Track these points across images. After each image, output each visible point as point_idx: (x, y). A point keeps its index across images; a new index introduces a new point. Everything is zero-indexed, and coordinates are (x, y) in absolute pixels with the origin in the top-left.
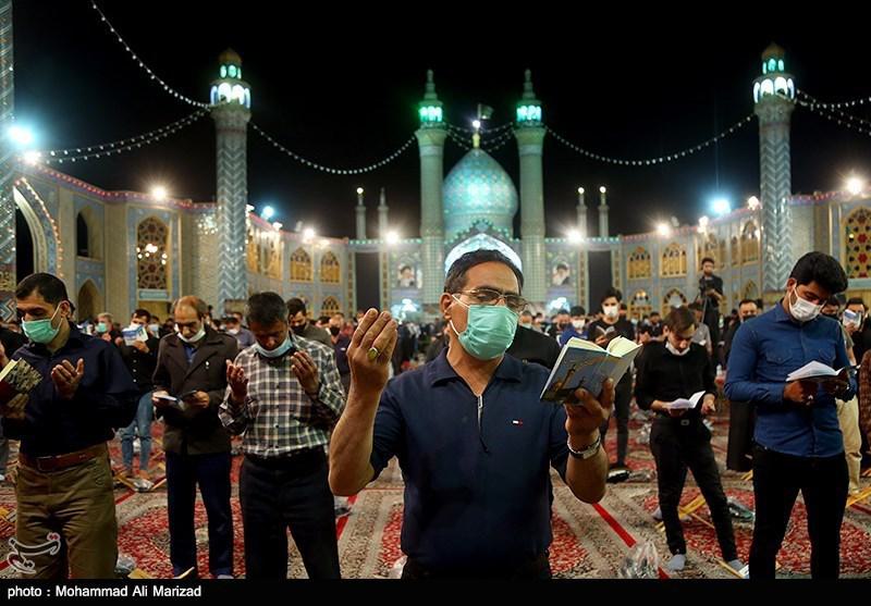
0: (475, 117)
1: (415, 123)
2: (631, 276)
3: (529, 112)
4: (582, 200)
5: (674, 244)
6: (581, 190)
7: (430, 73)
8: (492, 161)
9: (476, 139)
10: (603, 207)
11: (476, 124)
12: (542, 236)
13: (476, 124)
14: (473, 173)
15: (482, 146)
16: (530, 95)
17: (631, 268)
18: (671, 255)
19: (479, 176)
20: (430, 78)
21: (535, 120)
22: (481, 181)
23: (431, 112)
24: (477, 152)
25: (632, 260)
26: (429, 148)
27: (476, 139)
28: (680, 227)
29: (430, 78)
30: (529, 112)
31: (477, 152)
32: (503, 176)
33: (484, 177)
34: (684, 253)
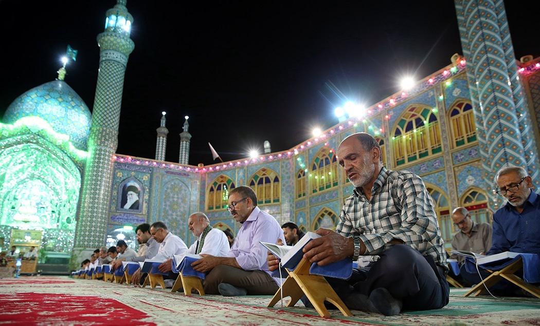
2: (210, 208)
4: (163, 122)
5: (264, 170)
6: (164, 113)
8: (73, 91)
9: (62, 73)
11: (65, 60)
12: (114, 152)
14: (48, 95)
15: (67, 79)
18: (261, 182)
19: (56, 99)
21: (125, 32)
22: (57, 103)
25: (212, 190)
27: (62, 73)
28: (272, 152)
32: (83, 107)
33: (60, 100)
34: (276, 180)
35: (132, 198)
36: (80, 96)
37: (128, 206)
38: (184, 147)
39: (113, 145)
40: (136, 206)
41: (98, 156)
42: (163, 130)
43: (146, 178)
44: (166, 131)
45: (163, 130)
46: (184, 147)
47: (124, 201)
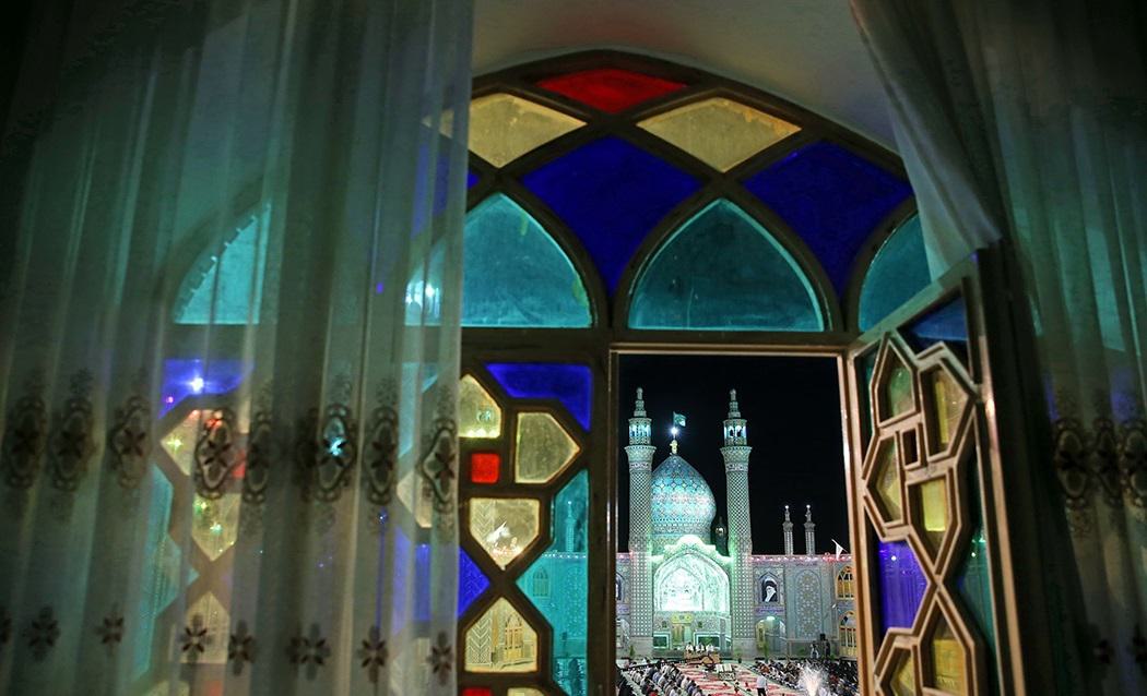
0: (670, 421)
1: (625, 439)
3: (736, 428)
7: (640, 391)
9: (674, 445)
10: (809, 525)
11: (674, 431)
13: (674, 431)
15: (680, 452)
16: (738, 414)
17: (840, 589)
20: (640, 396)
23: (640, 428)
24: (674, 460)
25: (840, 578)
26: (639, 455)
27: (674, 445)
29: (640, 396)
30: (736, 428)
31: (674, 460)
35: (771, 592)
36: (705, 479)
37: (767, 600)
38: (810, 538)
39: (749, 547)
40: (774, 598)
41: (740, 560)
42: (788, 525)
43: (780, 572)
44: (791, 525)
45: (788, 525)
46: (810, 538)
47: (765, 596)
